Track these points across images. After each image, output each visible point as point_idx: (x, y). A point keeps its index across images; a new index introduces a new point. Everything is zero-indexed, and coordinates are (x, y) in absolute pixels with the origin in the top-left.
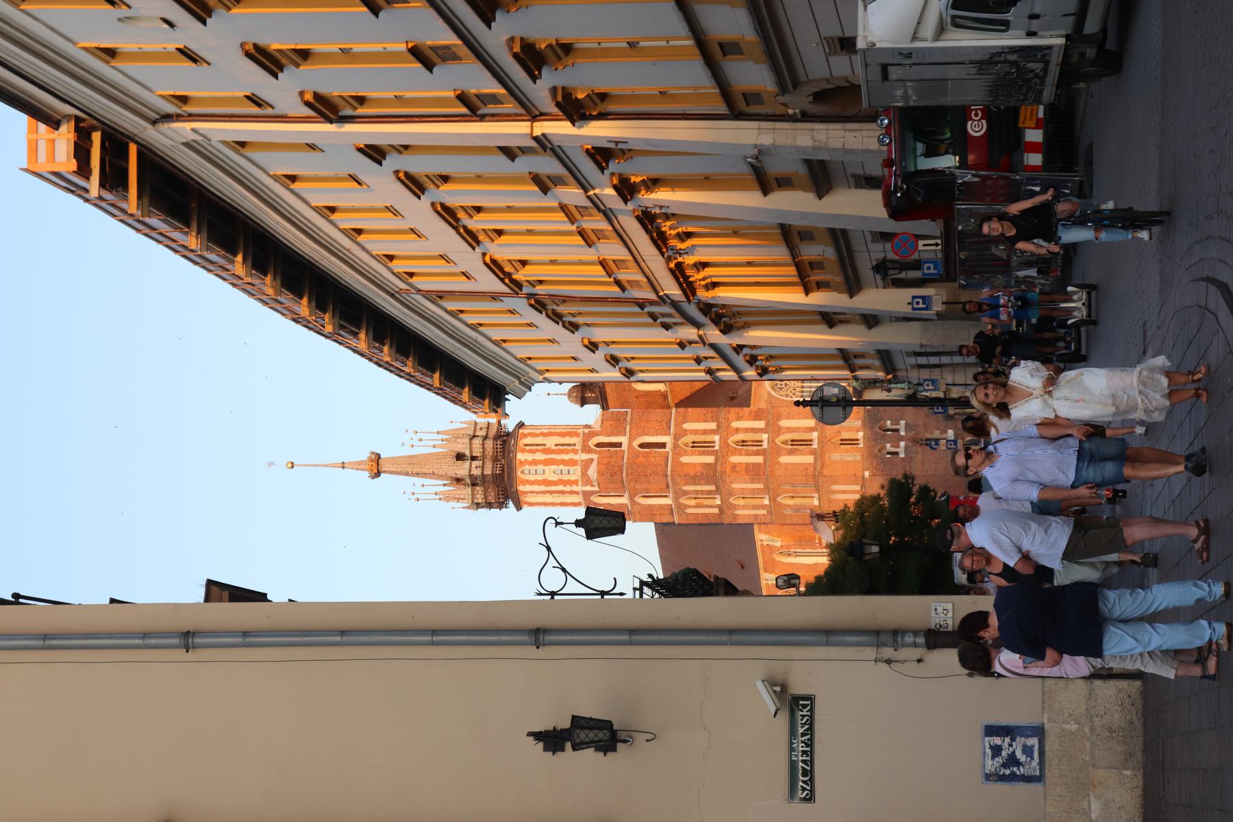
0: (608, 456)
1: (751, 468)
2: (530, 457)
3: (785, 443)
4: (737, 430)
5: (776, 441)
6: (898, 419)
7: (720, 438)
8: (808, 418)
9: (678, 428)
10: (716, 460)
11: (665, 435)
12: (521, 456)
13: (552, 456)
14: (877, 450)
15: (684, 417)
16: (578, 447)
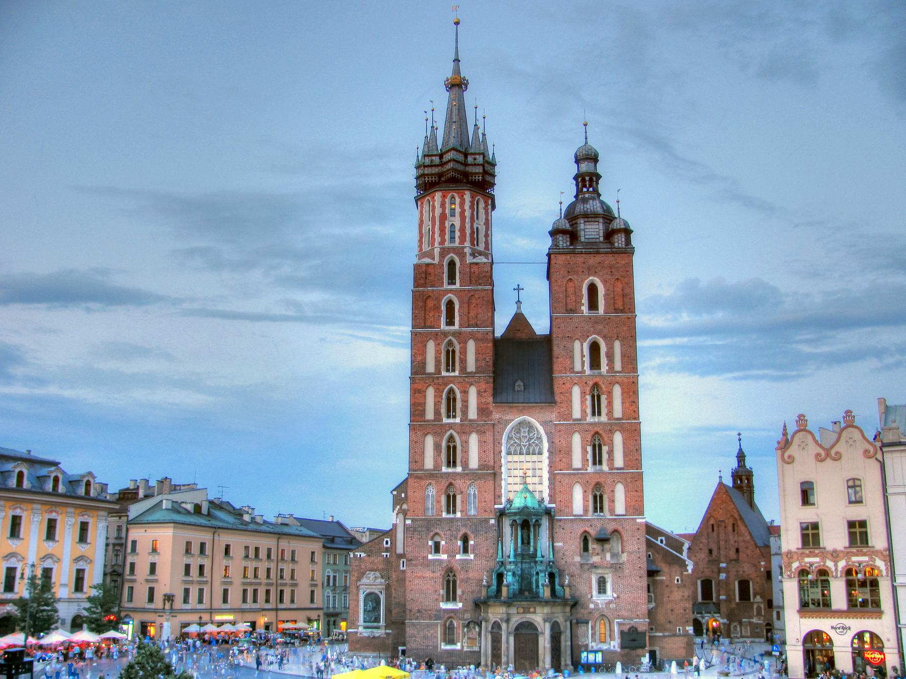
0: (436, 273)
1: (420, 408)
2: (437, 204)
3: (451, 438)
4: (465, 392)
5: (452, 431)
6: (476, 552)
7: (455, 377)
8: (479, 461)
9: (468, 335)
10: (430, 374)
11: (460, 323)
12: (438, 196)
13: (438, 223)
14: (437, 531)
15: (481, 339)
16: (447, 244)
